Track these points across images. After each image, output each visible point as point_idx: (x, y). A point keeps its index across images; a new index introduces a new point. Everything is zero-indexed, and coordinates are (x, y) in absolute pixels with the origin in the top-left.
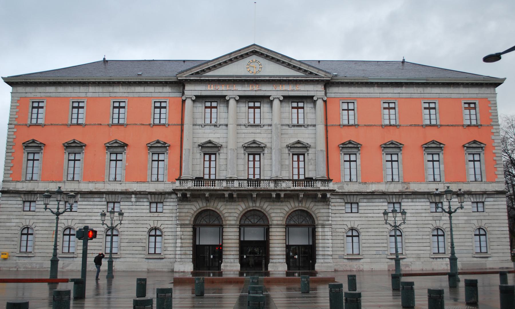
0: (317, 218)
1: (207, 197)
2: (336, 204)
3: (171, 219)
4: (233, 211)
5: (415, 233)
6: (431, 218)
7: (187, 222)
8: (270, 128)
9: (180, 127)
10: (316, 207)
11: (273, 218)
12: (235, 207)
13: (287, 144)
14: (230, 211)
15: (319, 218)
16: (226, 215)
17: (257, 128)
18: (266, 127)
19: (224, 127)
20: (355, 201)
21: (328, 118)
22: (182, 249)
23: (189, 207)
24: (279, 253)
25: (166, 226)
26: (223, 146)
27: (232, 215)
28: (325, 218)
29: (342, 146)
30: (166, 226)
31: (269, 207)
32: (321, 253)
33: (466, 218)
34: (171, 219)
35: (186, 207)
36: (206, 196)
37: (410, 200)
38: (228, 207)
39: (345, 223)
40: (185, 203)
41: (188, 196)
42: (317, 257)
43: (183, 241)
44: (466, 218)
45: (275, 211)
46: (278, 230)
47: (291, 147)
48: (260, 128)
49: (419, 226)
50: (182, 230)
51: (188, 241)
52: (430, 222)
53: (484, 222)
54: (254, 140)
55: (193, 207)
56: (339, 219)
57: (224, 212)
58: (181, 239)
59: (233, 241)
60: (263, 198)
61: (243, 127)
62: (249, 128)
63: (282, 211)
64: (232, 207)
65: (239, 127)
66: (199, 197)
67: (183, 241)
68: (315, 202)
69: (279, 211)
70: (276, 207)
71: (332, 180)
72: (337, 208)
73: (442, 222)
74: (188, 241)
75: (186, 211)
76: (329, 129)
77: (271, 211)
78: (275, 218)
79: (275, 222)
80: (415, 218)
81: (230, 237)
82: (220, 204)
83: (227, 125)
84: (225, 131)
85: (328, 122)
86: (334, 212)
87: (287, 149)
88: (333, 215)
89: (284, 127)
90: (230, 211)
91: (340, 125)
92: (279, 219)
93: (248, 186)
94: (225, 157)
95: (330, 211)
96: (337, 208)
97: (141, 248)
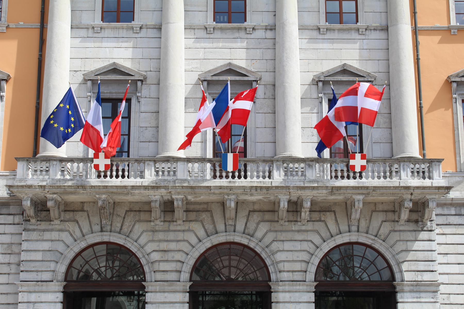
0: (399, 264)
1: (103, 208)
2: (447, 230)
4: (173, 246)
7: (46, 276)
8: (269, 34)
9: (37, 32)
10: (395, 236)
11: (281, 266)
12: (181, 236)
13: (315, 74)
14: (164, 246)
15: (405, 266)
16: (155, 256)
17: (237, 35)
18: (260, 34)
19: (152, 33)
21: (417, 10)
23: (55, 235)
26: (149, 81)
27: (169, 256)
28: (421, 266)
29: (458, 79)
31: (270, 237)
35: (47, 235)
36: (100, 203)
38: (161, 236)
40: (44, 225)
41: (50, 204)
45: (288, 246)
46: (296, 296)
47: (325, 83)
48: (242, 34)
54: (230, 64)
55: (65, 236)
56: (456, 269)
57: (149, 248)
60: (254, 211)
61: (202, 33)
62: (218, 34)
63: (306, 246)
64: (171, 236)
65: (191, 34)
66: (83, 210)
68: (394, 221)
69: (298, 246)
70: (289, 235)
71: (440, 161)
72: (450, 239)
75: (46, 246)
76: (420, 38)
77: (275, 246)
78: (287, 266)
79: (285, 276)
82: (139, 228)
83: (159, 28)
84: (154, 43)
85: (418, 21)
86: (443, 249)
87: (314, 87)
88: (441, 259)
89: (308, 34)
90: (164, 246)
91: (449, 29)
92: (298, 266)
93: (215, 177)
94: (154, 109)
95: (433, 246)
96: (450, 239)
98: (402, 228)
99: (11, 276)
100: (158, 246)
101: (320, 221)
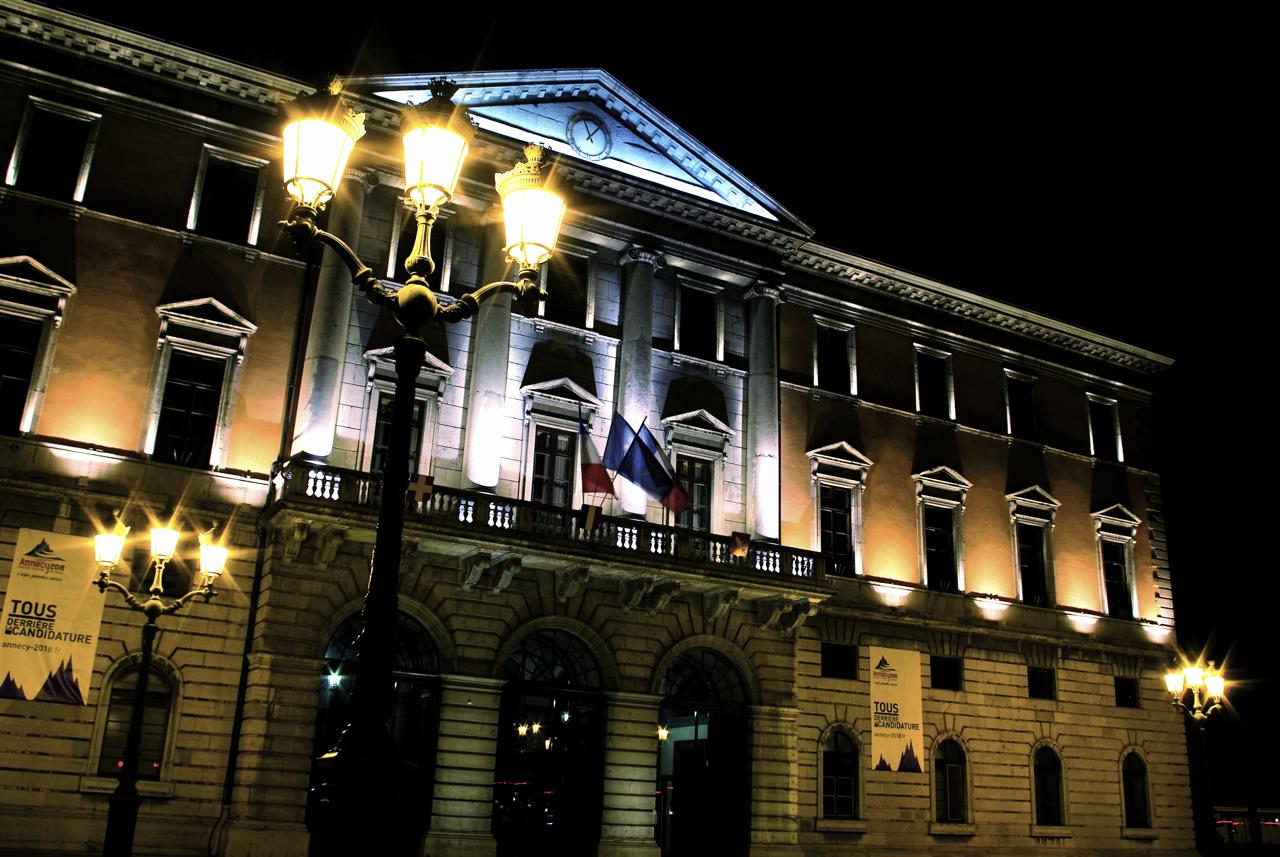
3: (220, 629)
5: (995, 759)
6: (1030, 715)
20: (847, 642)
22: (269, 762)
24: (636, 802)
25: (196, 659)
30: (196, 659)
32: (764, 808)
33: (1103, 722)
34: (220, 629)
37: (983, 655)
39: (821, 709)
42: (754, 824)
43: (276, 730)
44: (1103, 722)
49: (1007, 736)
50: (280, 679)
51: (297, 731)
52: (1030, 727)
53: (1142, 736)
58: (269, 718)
59: (475, 746)
67: (276, 730)
73: (1056, 730)
74: (297, 731)
80: (993, 712)
81: (466, 729)
90: (473, 624)
97: (66, 747)
98: (764, 636)
99: (228, 642)
100: (465, 622)
101: (671, 613)
